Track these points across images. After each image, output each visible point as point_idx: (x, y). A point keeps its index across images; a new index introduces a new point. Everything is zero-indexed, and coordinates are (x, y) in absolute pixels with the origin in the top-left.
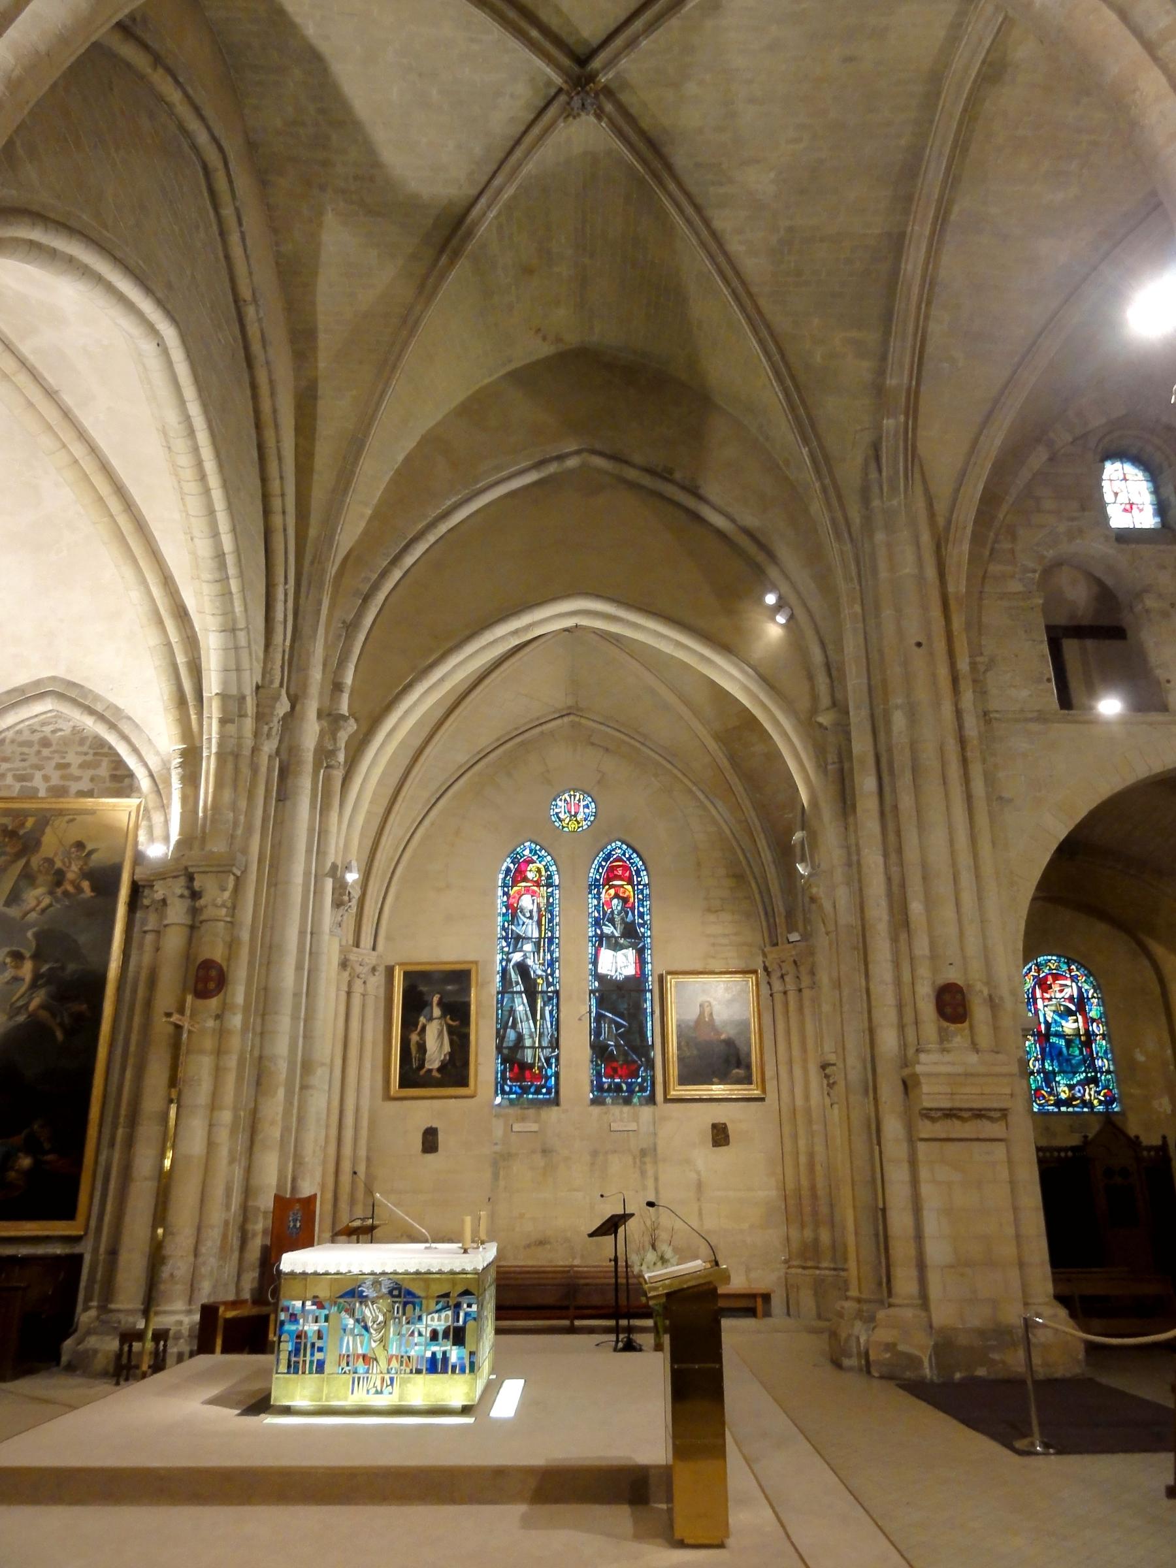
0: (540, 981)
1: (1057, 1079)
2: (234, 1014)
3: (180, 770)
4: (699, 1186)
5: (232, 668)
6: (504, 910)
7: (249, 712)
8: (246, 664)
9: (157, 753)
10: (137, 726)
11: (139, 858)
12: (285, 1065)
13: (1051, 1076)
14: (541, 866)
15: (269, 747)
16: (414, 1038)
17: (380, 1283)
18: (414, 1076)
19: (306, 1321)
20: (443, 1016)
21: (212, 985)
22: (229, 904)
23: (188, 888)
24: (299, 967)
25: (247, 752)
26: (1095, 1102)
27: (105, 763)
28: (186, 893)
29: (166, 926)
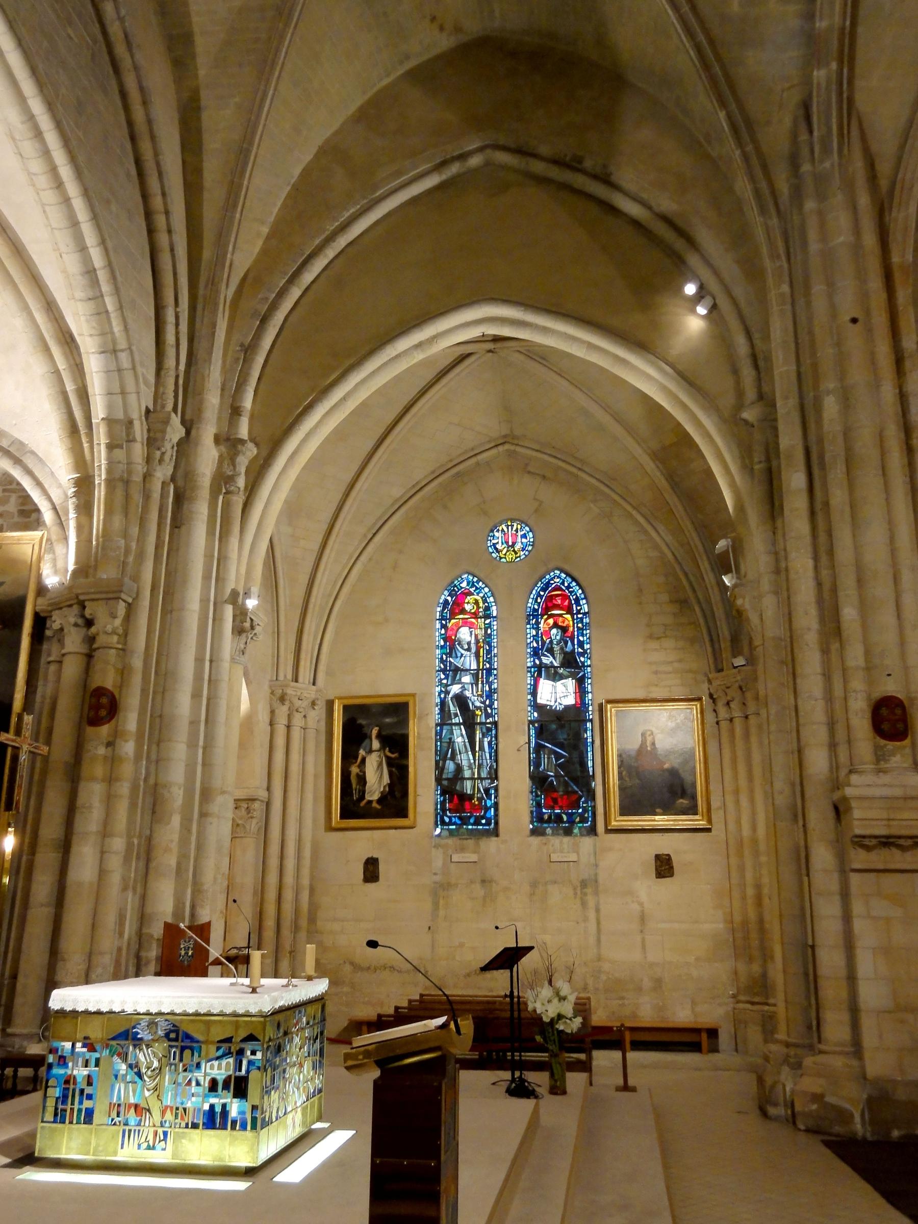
0: (478, 712)
2: (126, 741)
3: (74, 499)
4: (643, 919)
5: (118, 391)
6: (442, 643)
7: (138, 436)
8: (130, 386)
9: (60, 486)
10: (40, 460)
11: (41, 590)
12: (181, 792)
14: (478, 598)
15: (163, 472)
16: (354, 770)
17: (156, 1024)
18: (354, 807)
19: (75, 1064)
20: (382, 748)
21: (103, 713)
22: (120, 631)
23: (83, 616)
24: (196, 695)
25: (137, 478)
27: (13, 499)
28: (80, 621)
29: (63, 655)
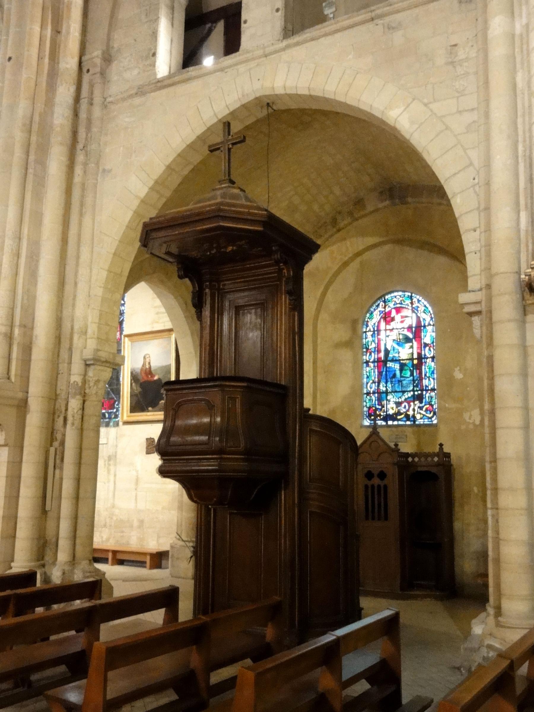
1: (389, 398)
13: (384, 395)
26: (418, 416)
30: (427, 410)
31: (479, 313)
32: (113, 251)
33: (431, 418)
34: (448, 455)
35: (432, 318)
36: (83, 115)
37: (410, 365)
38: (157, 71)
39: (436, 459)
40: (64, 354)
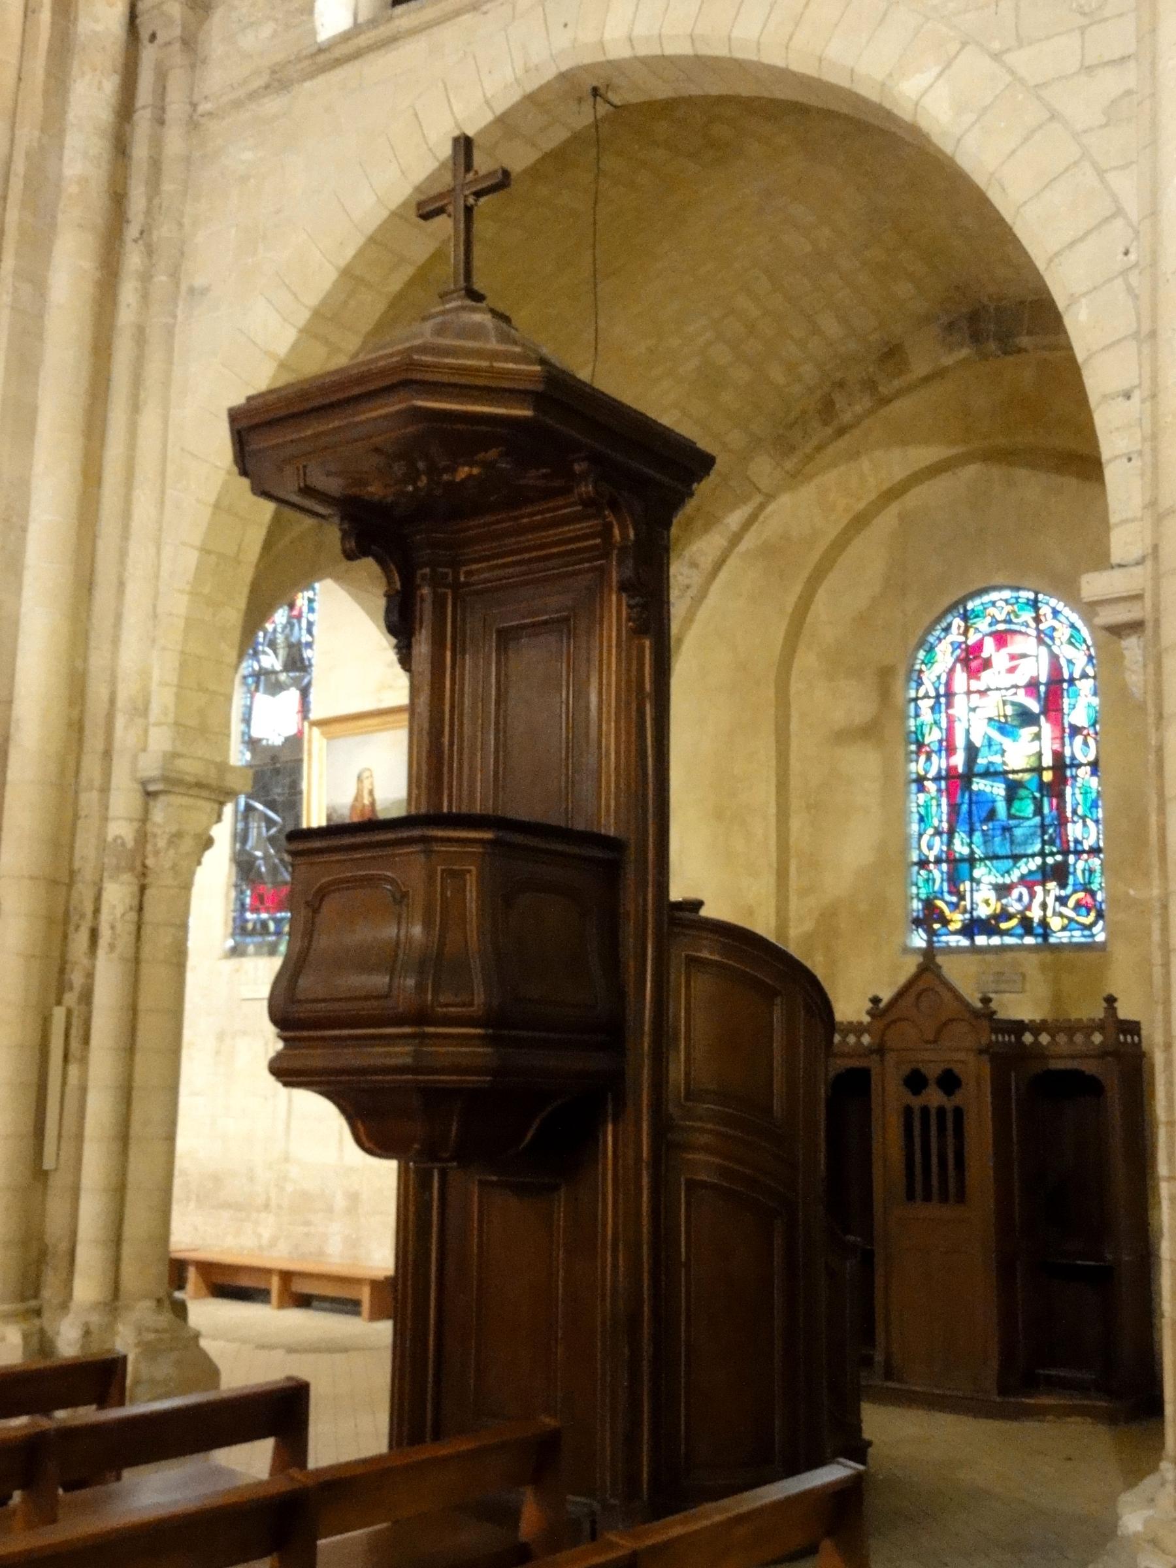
1: (977, 873)
13: (965, 867)
26: (1055, 923)
30: (1078, 905)
31: (1136, 627)
32: (212, 499)
33: (1089, 927)
34: (1133, 1028)
35: (1090, 658)
36: (140, 151)
37: (1033, 786)
38: (318, 24)
39: (1097, 1038)
40: (91, 767)
